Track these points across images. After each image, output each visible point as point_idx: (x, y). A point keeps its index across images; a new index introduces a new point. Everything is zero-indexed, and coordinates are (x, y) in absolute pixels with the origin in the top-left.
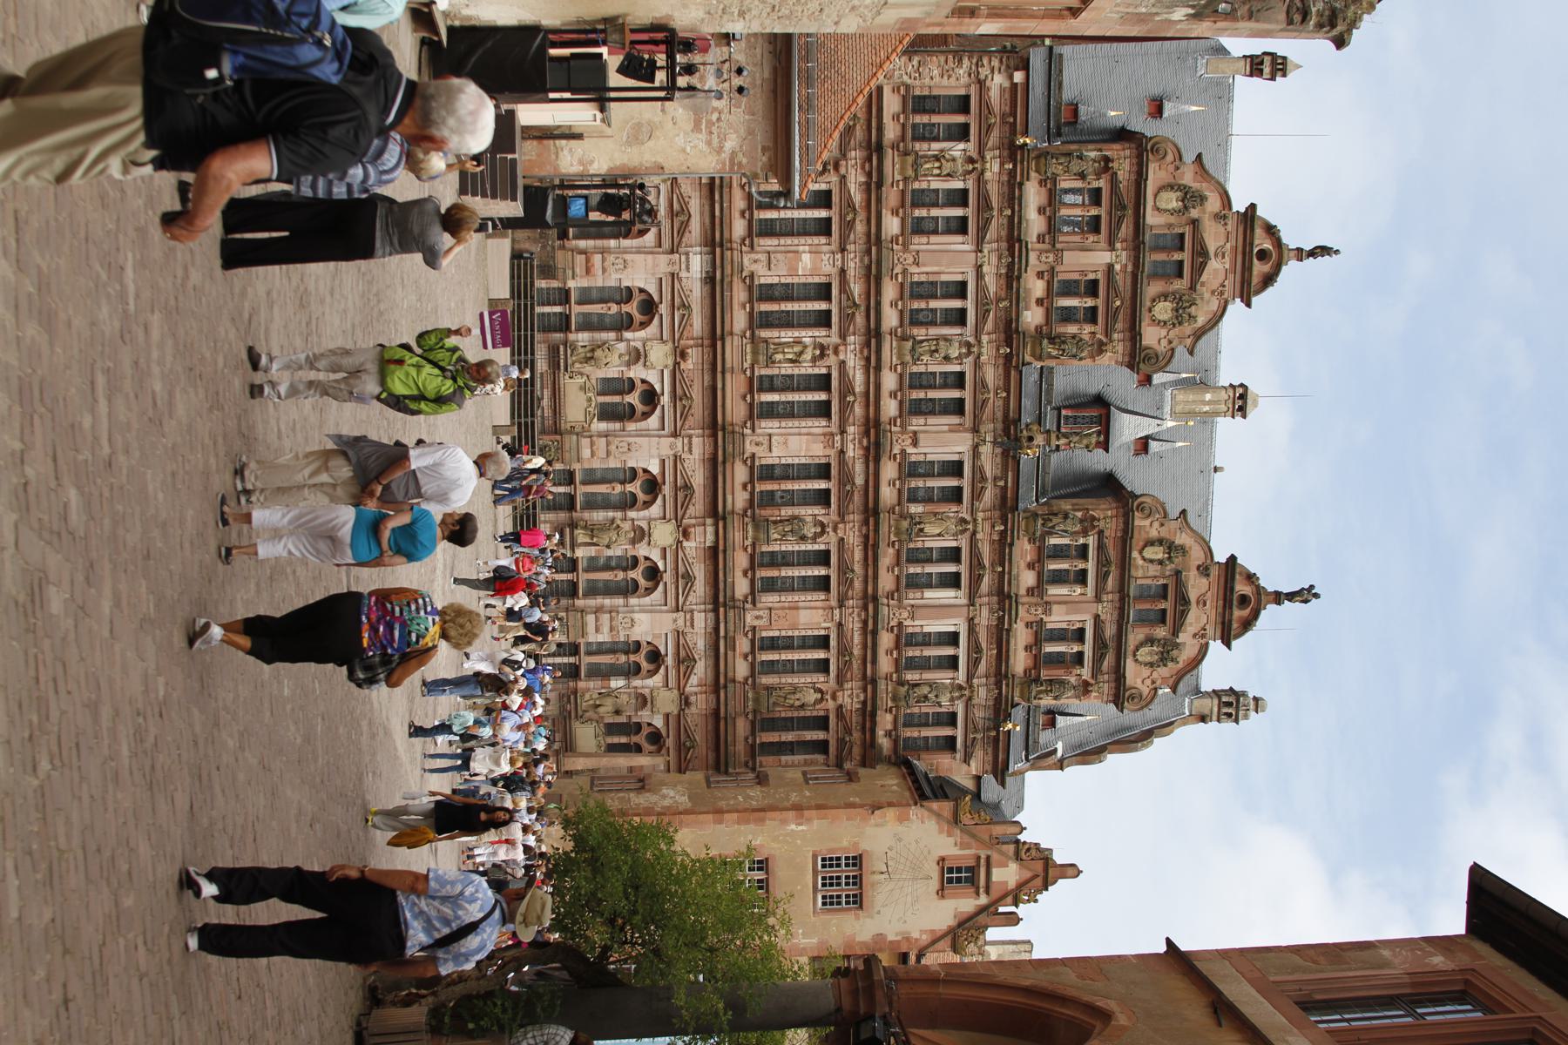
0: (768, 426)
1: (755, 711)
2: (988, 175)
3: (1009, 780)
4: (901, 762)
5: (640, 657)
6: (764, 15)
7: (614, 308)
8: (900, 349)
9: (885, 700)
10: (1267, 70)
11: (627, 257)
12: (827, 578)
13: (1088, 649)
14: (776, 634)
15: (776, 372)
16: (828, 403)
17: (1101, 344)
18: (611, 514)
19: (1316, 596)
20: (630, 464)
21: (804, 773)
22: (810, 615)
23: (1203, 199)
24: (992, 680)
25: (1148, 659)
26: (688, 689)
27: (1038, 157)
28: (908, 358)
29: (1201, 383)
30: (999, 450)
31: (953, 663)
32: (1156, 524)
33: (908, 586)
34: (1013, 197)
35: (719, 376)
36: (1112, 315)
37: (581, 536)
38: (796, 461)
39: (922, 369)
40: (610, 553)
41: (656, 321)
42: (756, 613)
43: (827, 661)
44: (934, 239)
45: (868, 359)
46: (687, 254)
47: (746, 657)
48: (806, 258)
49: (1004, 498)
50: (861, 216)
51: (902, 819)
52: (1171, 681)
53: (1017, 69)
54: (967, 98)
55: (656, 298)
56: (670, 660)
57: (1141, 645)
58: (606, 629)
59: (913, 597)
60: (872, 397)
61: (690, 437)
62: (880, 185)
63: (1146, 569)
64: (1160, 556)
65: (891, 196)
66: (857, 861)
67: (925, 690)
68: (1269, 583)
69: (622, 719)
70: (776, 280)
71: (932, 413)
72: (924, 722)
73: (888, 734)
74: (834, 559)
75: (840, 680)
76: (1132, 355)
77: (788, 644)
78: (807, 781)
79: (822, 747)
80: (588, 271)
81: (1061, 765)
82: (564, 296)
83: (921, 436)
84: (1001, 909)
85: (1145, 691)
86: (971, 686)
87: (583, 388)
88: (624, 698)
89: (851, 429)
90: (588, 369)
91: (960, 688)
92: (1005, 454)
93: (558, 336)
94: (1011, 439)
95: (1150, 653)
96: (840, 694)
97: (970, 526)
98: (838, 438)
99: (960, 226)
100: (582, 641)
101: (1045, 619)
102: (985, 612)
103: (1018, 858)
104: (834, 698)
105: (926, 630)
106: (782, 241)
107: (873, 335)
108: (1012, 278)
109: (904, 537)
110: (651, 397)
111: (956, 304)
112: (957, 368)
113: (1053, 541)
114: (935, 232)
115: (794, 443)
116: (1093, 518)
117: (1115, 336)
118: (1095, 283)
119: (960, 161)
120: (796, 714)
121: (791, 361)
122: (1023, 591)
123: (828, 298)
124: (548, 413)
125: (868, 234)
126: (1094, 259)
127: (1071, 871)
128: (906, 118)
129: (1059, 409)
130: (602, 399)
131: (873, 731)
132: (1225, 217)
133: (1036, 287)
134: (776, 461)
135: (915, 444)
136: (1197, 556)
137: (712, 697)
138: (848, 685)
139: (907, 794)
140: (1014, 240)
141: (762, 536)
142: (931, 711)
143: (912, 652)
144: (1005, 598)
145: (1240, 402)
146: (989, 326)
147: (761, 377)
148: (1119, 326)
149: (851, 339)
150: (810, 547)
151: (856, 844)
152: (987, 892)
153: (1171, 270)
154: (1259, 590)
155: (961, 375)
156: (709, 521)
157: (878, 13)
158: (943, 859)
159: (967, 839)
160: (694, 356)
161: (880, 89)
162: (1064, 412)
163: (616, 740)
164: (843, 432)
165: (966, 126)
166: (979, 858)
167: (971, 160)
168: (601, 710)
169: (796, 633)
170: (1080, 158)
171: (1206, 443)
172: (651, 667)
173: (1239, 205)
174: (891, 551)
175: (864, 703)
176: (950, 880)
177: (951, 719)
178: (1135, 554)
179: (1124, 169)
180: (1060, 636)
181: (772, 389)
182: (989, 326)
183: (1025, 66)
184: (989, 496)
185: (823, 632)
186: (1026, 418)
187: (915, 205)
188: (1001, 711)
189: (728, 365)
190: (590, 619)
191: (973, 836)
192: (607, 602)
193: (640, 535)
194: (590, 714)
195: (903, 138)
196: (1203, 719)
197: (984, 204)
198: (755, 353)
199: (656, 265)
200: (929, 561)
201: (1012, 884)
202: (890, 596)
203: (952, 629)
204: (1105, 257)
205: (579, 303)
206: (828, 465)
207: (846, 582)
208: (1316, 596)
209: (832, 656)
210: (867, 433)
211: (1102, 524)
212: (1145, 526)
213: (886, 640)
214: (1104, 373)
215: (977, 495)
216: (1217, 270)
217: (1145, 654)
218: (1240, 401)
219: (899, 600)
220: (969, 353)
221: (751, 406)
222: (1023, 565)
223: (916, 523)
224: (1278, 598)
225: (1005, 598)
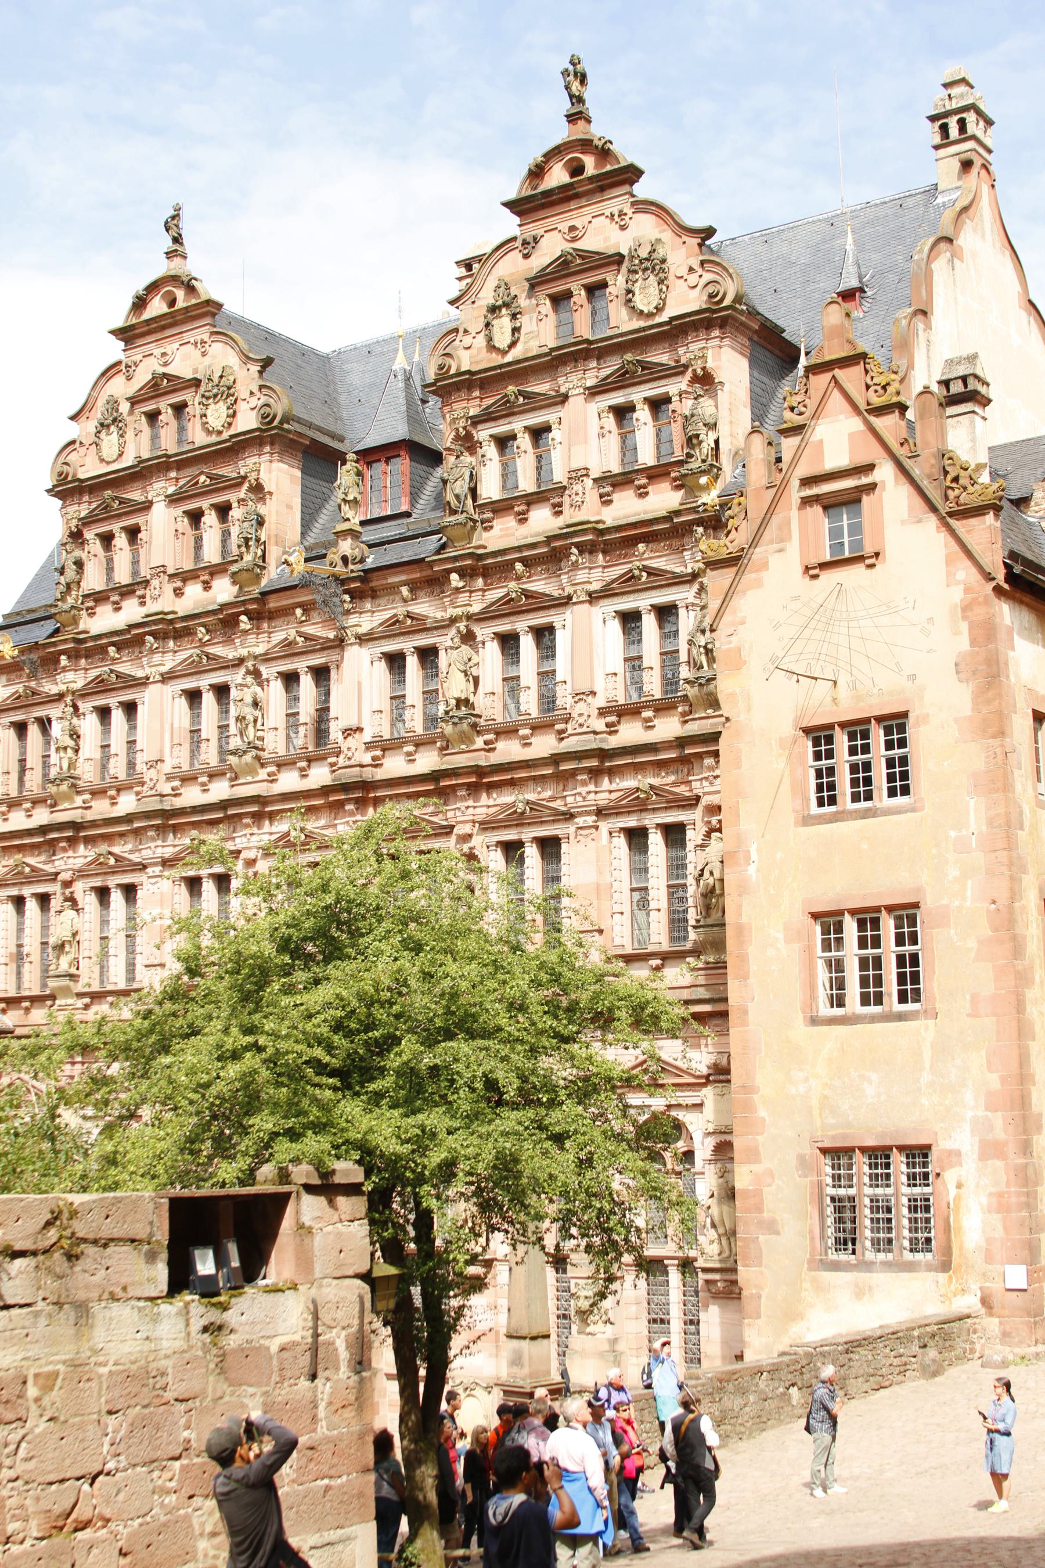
32: (467, 340)
51: (738, 662)
66: (821, 736)
101: (595, 474)
152: (870, 468)
166: (806, 502)
174: (501, 745)
176: (857, 544)
201: (856, 424)
217: (646, 298)
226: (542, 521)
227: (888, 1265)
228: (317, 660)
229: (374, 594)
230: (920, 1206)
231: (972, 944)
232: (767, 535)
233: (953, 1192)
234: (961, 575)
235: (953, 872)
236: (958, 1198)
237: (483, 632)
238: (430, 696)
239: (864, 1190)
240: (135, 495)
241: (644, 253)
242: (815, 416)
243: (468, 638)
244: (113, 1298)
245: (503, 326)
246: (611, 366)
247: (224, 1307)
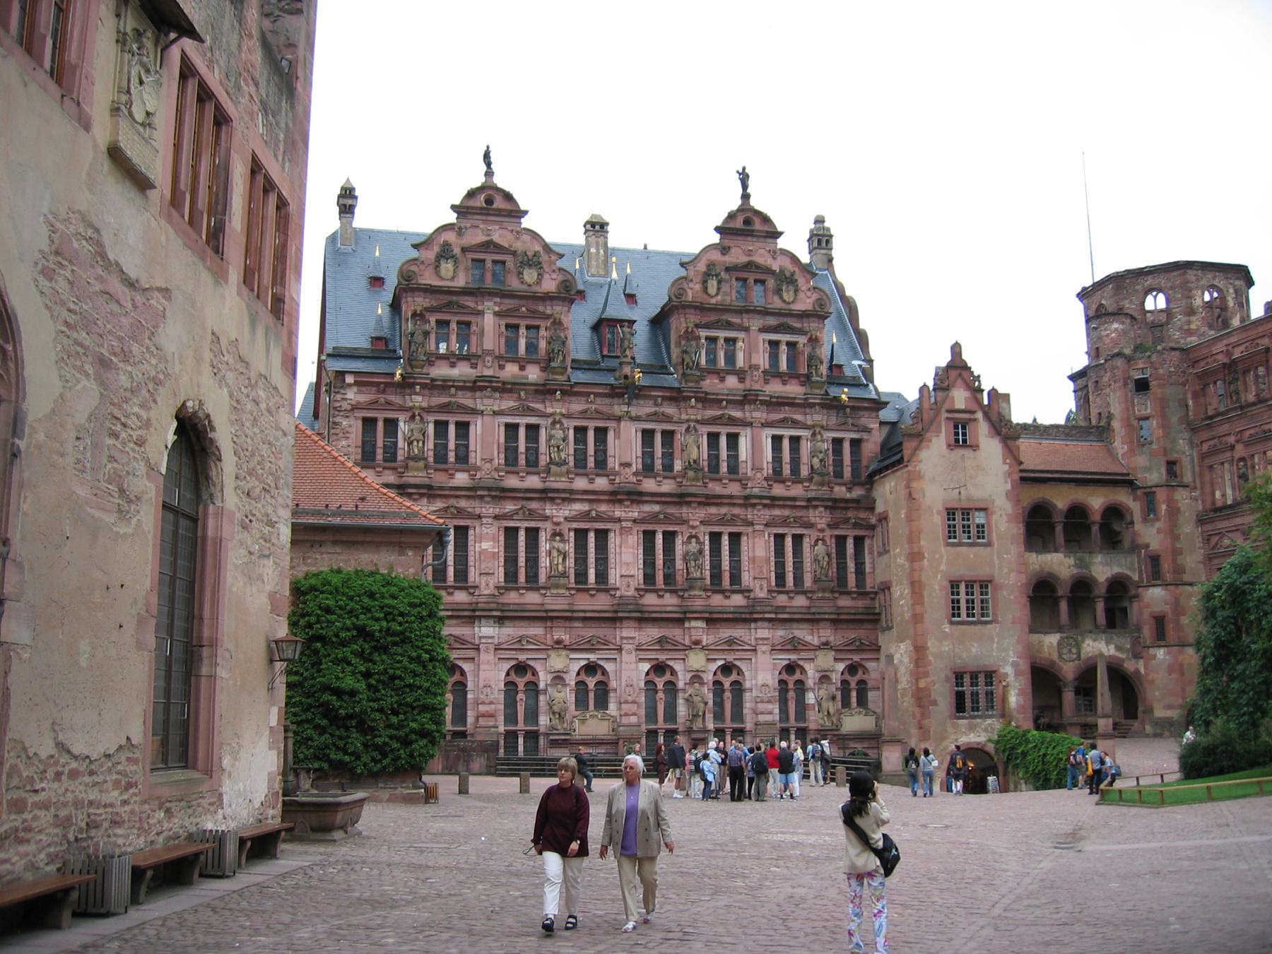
0: (614, 577)
1: (833, 592)
2: (424, 404)
3: (884, 399)
4: (870, 480)
5: (791, 680)
6: (273, 501)
7: (521, 696)
8: (556, 475)
9: (823, 492)
10: (349, 202)
11: (481, 684)
12: (731, 534)
13: (784, 338)
14: (773, 574)
15: (572, 571)
16: (597, 531)
17: (554, 323)
18: (680, 701)
19: (744, 169)
20: (642, 684)
21: (880, 554)
22: (757, 548)
23: (446, 246)
24: (808, 410)
25: (792, 293)
26: (816, 642)
27: (412, 367)
28: (564, 468)
29: (583, 253)
30: (635, 402)
31: (795, 440)
32: (691, 285)
33: (737, 473)
34: (443, 386)
35: (576, 615)
36: (534, 314)
37: (698, 725)
38: (641, 556)
39: (572, 458)
40: (711, 703)
41: (531, 663)
42: (757, 590)
43: (794, 536)
44: (472, 447)
45: (564, 499)
46: (480, 638)
47: (791, 598)
48: (485, 545)
49: (671, 399)
50: (453, 502)
52: (809, 277)
53: (344, 381)
54: (365, 420)
55: (513, 663)
56: (793, 657)
57: (781, 298)
58: (770, 706)
59: (746, 469)
60: (592, 496)
61: (622, 638)
62: (430, 487)
63: (726, 294)
64: (715, 283)
65: (439, 479)
66: (951, 513)
67: (816, 461)
68: (735, 203)
69: (839, 694)
70: (502, 570)
71: (605, 452)
72: (838, 463)
73: (849, 490)
74: (716, 529)
75: (810, 526)
76: (563, 299)
77: (780, 565)
78: (887, 552)
79: (859, 541)
80: (492, 716)
81: (870, 362)
82: (511, 736)
83: (623, 460)
84: (986, 402)
85: (815, 296)
86: (813, 426)
87: (583, 721)
88: (823, 693)
89: (617, 514)
90: (568, 717)
91: (814, 435)
92: (637, 397)
93: (542, 741)
94: (627, 391)
95: (788, 291)
96: (819, 526)
97: (692, 424)
98: (624, 524)
99: (463, 428)
100: (778, 725)
102: (755, 414)
103: (947, 389)
104: (822, 531)
105: (770, 459)
106: (471, 563)
107: (546, 495)
108: (506, 388)
109: (700, 475)
110: (591, 668)
111: (522, 432)
112: (571, 432)
113: (703, 362)
114: (467, 446)
115: (626, 559)
116: (686, 332)
117: (549, 312)
118: (507, 326)
119: (413, 426)
120: (834, 560)
121: (564, 559)
122: (741, 386)
123: (516, 529)
124: (602, 750)
125: (468, 497)
126: (489, 324)
127: (956, 349)
128: (379, 466)
129: (603, 357)
130: (591, 706)
131: (846, 501)
132: (460, 228)
133: (511, 370)
134: (641, 572)
135: (628, 465)
136: (716, 256)
137: (822, 624)
138: (813, 520)
139: (899, 473)
140: (475, 386)
141: (699, 583)
142: (831, 458)
143: (787, 470)
144: (748, 399)
145: (597, 227)
146: (539, 406)
147: (576, 583)
148: (541, 308)
149: (548, 512)
150: (707, 548)
152: (973, 412)
153: (498, 268)
154: (740, 210)
155: (576, 429)
156: (687, 625)
157: (275, 388)
158: (949, 446)
159: (933, 427)
160: (560, 634)
162: (605, 353)
163: (854, 700)
164: (619, 520)
165: (386, 421)
166: (948, 418)
167: (413, 418)
168: (832, 711)
169: (773, 559)
170: (412, 334)
171: (625, 254)
172: (798, 672)
173: (452, 218)
175: (826, 507)
176: (965, 441)
177: (837, 442)
178: (713, 301)
179: (421, 302)
180: (774, 357)
181: (585, 574)
182: (539, 406)
183: (341, 374)
184: (670, 410)
185: (772, 539)
186: (612, 381)
187: (445, 461)
188: (833, 405)
189: (566, 607)
190: (762, 718)
191: (931, 423)
192: (748, 705)
193: (696, 678)
194: (834, 719)
195: (395, 469)
196: (830, 260)
197: (445, 408)
198: (557, 586)
199: (488, 662)
200: (717, 457)
201: (966, 394)
202: (745, 487)
203: (770, 440)
204: (489, 320)
205: (516, 723)
206: (644, 532)
207: (733, 520)
208: (744, 169)
209: (789, 532)
210: (621, 502)
211: (691, 325)
212: (693, 292)
213: (778, 490)
214: (578, 324)
215: (668, 419)
216: (499, 236)
217: (788, 296)
218: (597, 227)
219: (748, 479)
220: (560, 422)
221: (598, 590)
222: (721, 386)
223: (692, 465)
224: (746, 197)
225: (748, 399)
228: (600, 424)
230: (990, 695)
237: (704, 430)
239: (967, 688)
246: (772, 321)
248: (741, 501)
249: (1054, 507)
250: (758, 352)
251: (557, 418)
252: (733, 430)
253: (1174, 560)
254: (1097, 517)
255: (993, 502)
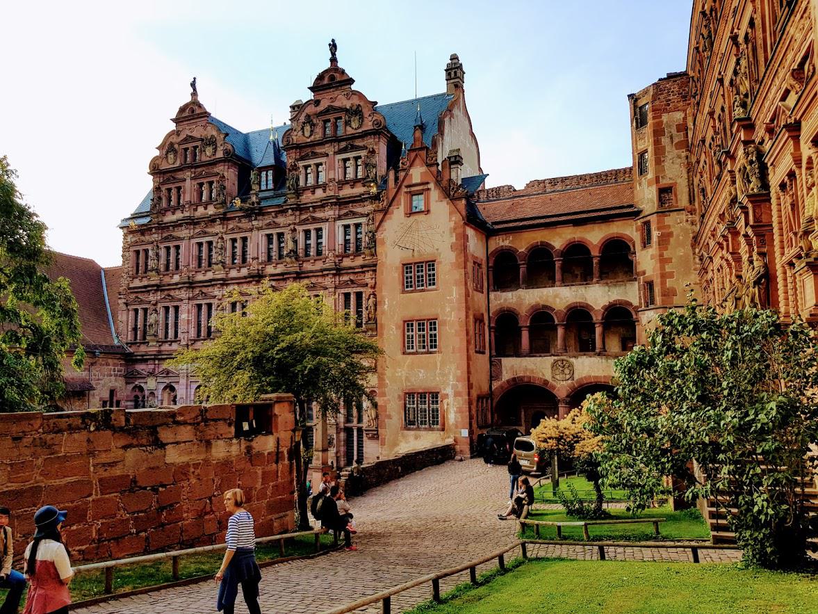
32: (295, 133)
45: (222, 285)
51: (383, 243)
59: (326, 252)
65: (167, 280)
68: (327, 65)
108: (192, 222)
151: (397, 268)
152: (428, 183)
161: (130, 289)
166: (406, 192)
173: (173, 126)
178: (309, 140)
184: (281, 220)
201: (424, 169)
204: (188, 181)
208: (333, 41)
210: (250, 282)
212: (297, 138)
213: (347, 262)
224: (334, 60)
225: (323, 205)
226: (319, 193)
227: (425, 429)
229: (263, 214)
231: (453, 331)
232: (394, 203)
233: (446, 407)
234: (454, 219)
235: (448, 310)
236: (447, 409)
237: (300, 228)
238: (280, 249)
240: (180, 175)
241: (354, 108)
242: (411, 166)
243: (294, 230)
244: (218, 438)
245: (308, 128)
246: (343, 144)
247: (252, 440)
248: (321, 274)
249: (553, 247)
250: (335, 170)
251: (220, 235)
252: (318, 226)
253: (663, 283)
254: (595, 253)
255: (440, 254)
